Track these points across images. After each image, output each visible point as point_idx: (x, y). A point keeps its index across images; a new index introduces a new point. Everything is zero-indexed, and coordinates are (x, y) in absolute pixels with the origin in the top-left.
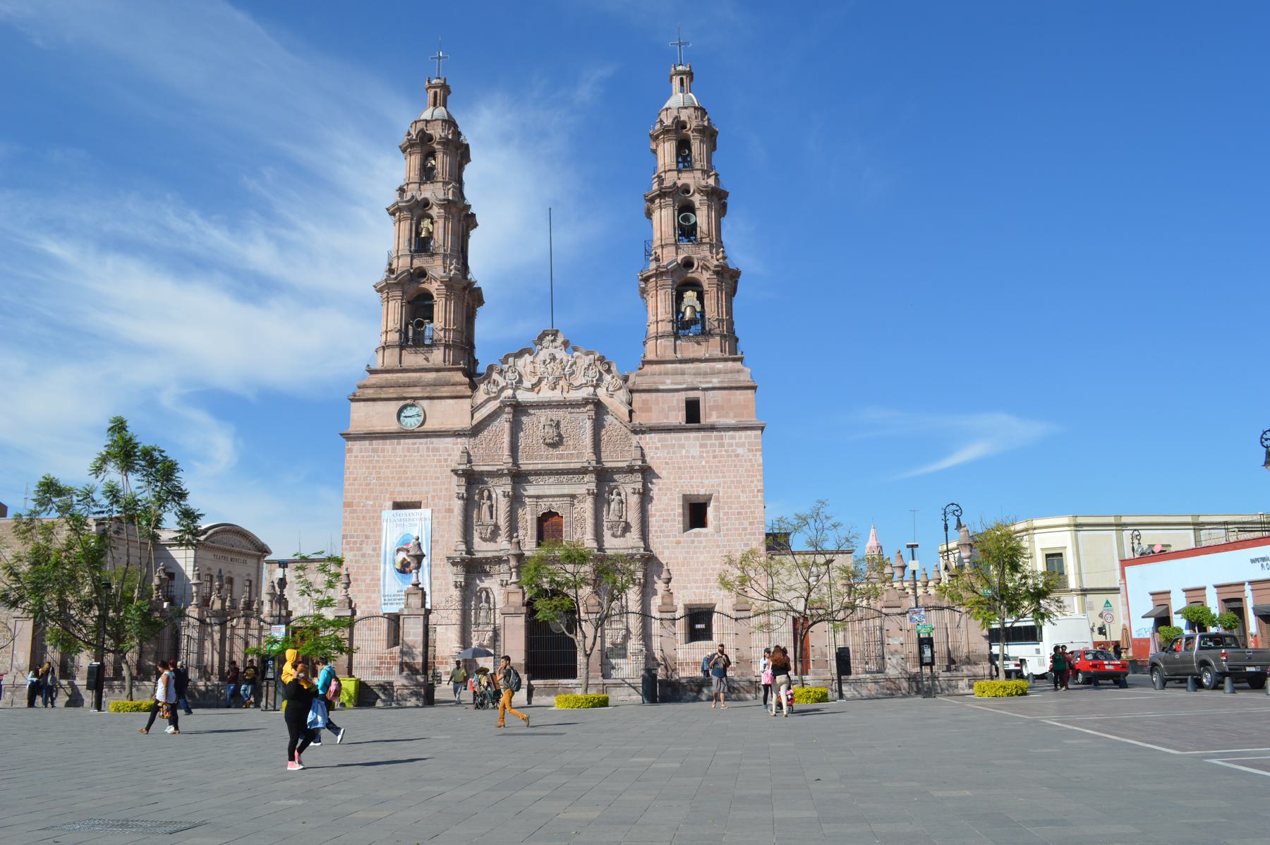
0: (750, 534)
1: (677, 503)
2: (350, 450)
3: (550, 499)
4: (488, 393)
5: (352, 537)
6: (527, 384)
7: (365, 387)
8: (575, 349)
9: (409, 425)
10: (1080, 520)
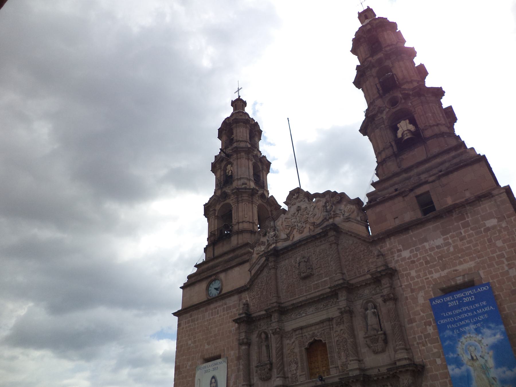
3: (313, 328)
6: (283, 236)
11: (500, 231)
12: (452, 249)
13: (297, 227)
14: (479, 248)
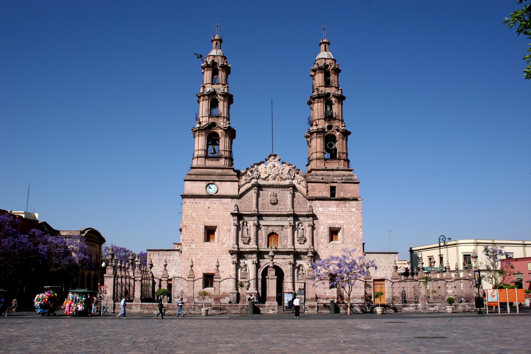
1: (326, 230)
2: (185, 203)
3: (273, 227)
4: (246, 180)
5: (186, 240)
6: (263, 176)
7: (190, 175)
8: (283, 163)
9: (211, 192)
10: (478, 241)
11: (355, 214)
12: (338, 214)
13: (271, 175)
14: (347, 217)
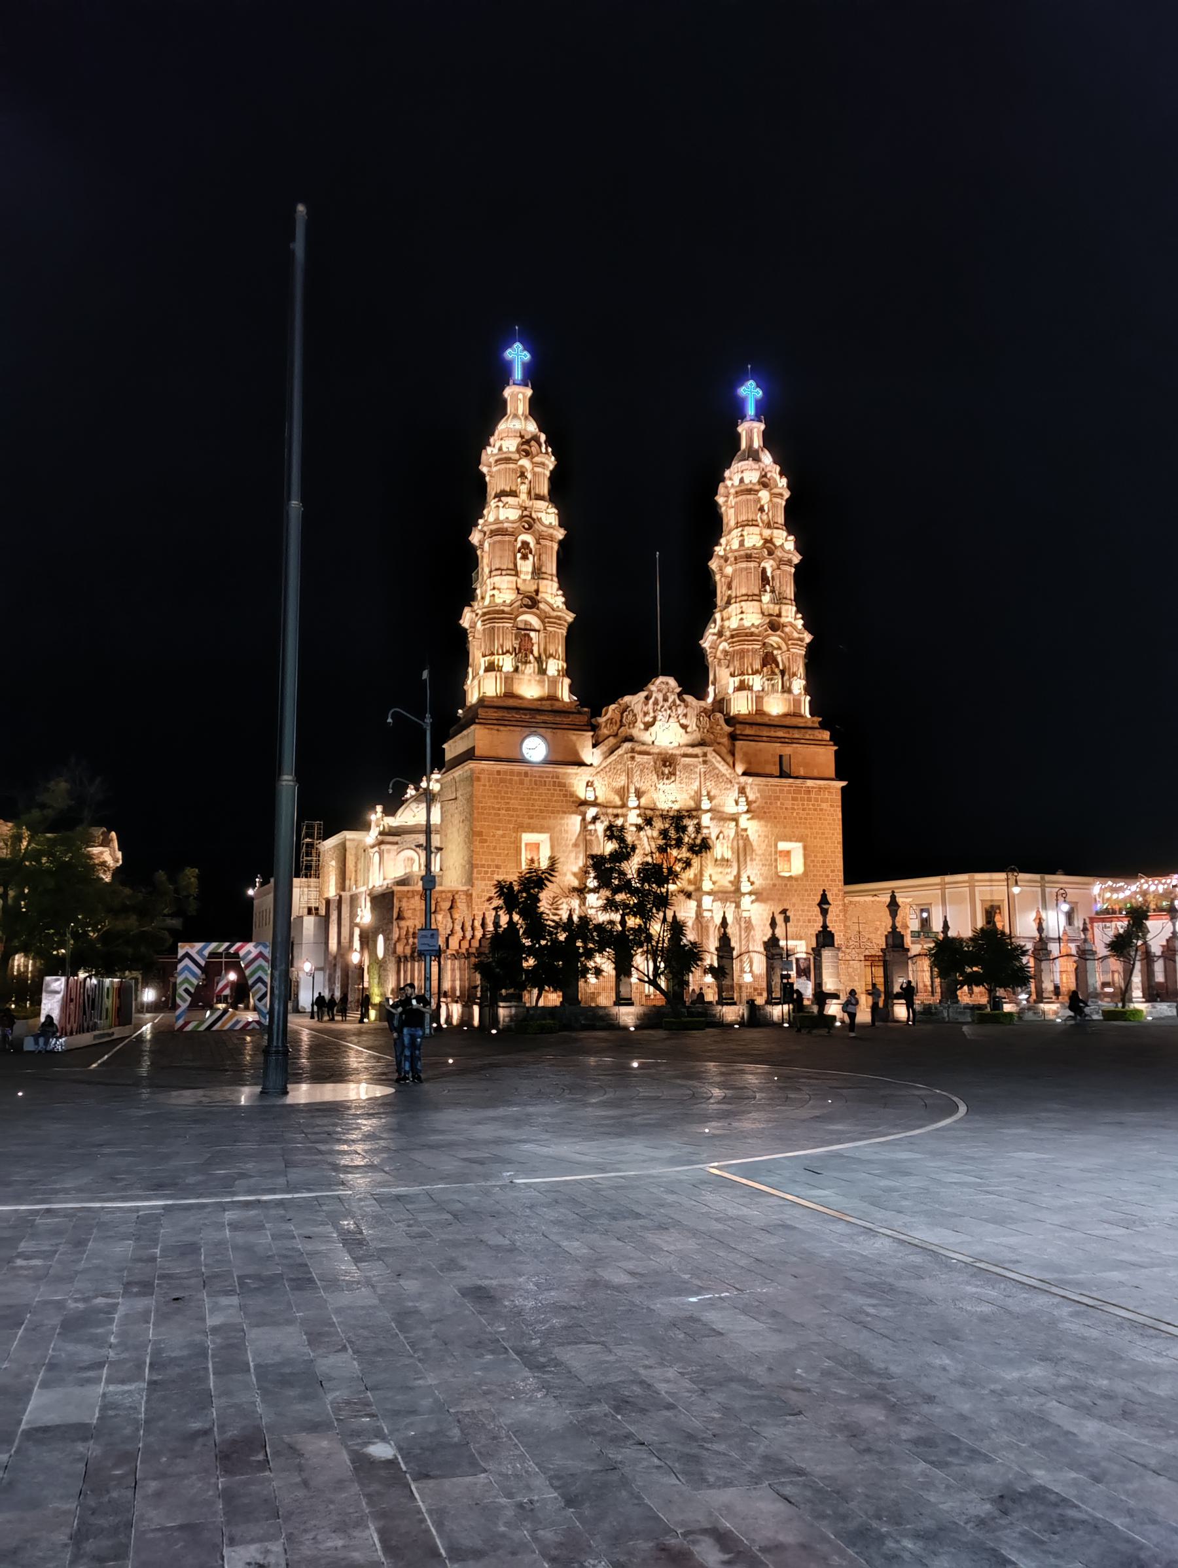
0: (832, 881)
5: (483, 866)
